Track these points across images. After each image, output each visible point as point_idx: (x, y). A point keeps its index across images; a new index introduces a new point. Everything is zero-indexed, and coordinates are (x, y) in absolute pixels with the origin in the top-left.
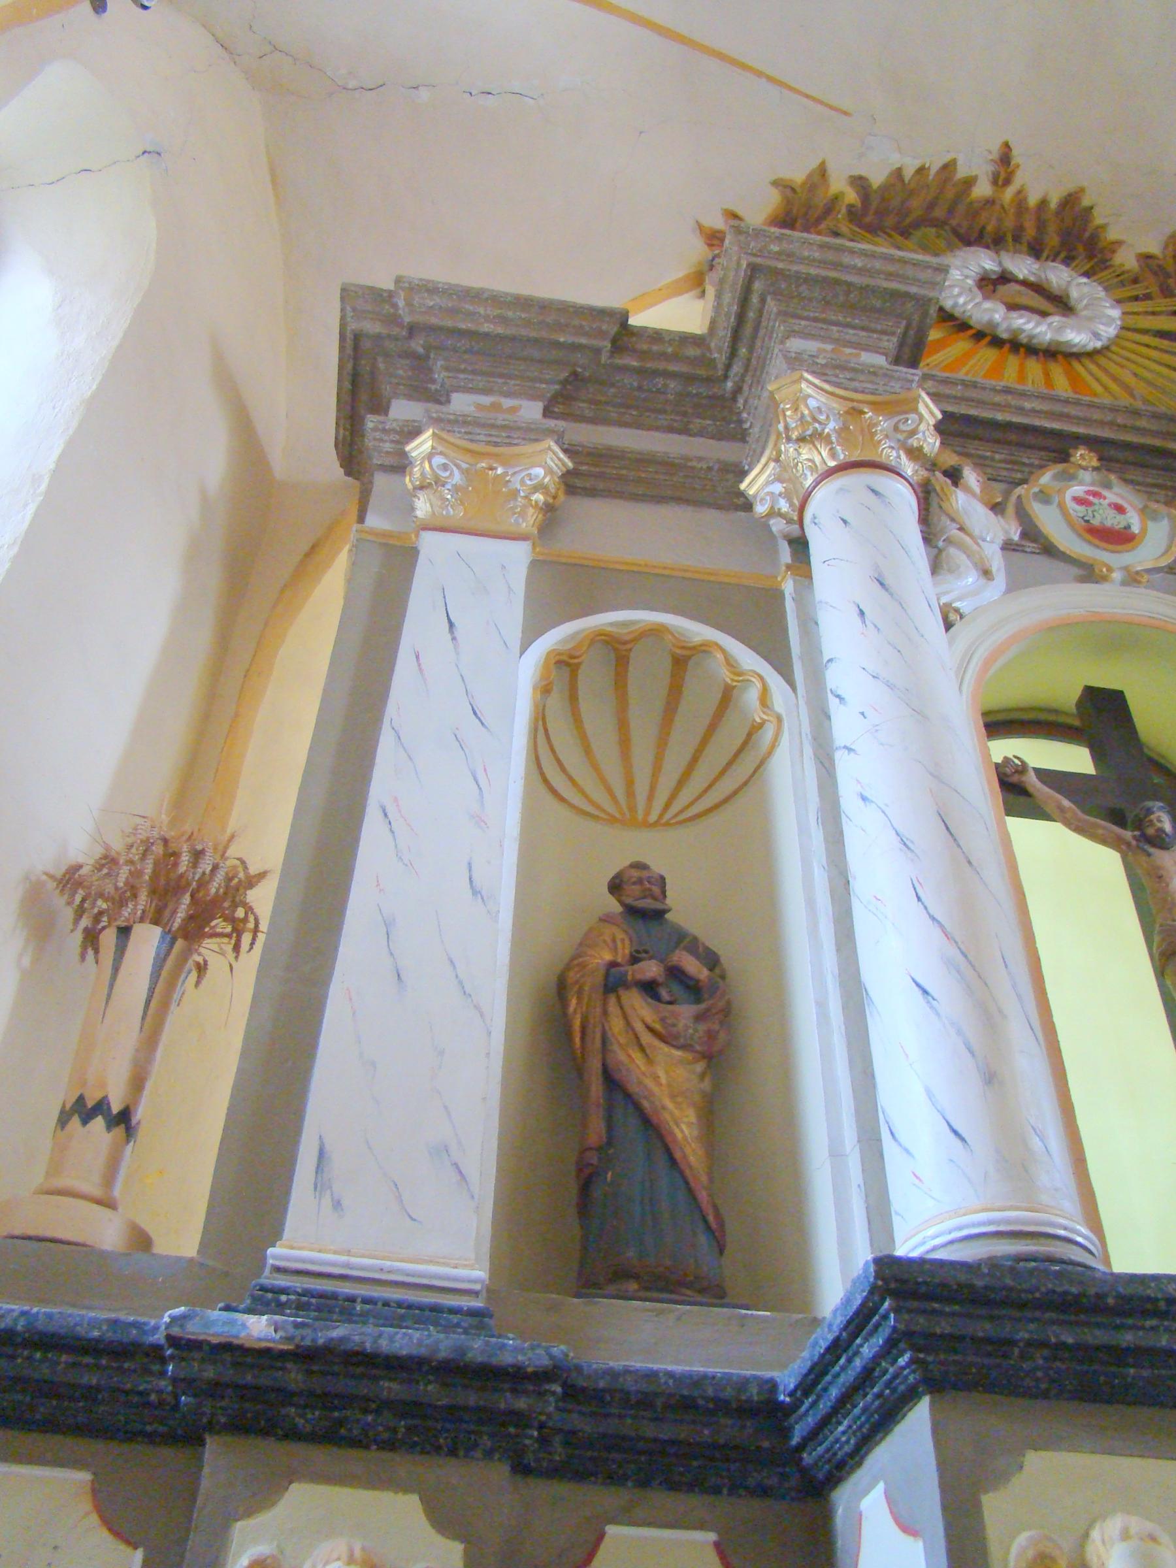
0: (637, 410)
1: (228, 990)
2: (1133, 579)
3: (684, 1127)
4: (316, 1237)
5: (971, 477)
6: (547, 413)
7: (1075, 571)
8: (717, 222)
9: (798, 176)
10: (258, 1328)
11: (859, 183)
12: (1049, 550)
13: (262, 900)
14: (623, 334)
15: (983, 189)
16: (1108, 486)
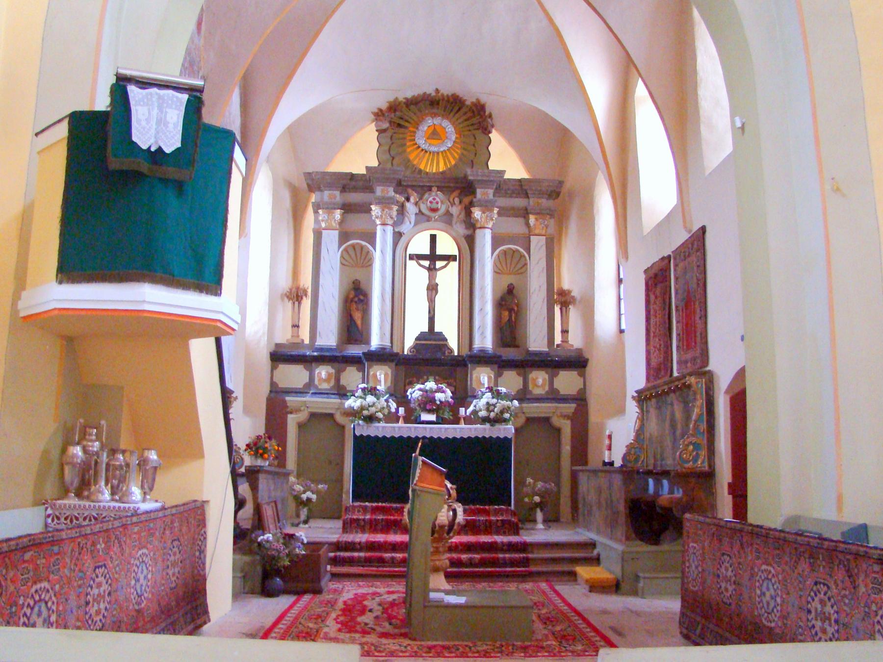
0: (355, 189)
1: (307, 303)
2: (436, 220)
3: (359, 322)
4: (320, 342)
5: (412, 200)
6: (341, 192)
7: (426, 218)
8: (376, 111)
9: (392, 100)
10: (315, 354)
11: (406, 98)
12: (423, 214)
13: (309, 291)
14: (352, 176)
15: (433, 94)
16: (437, 195)
